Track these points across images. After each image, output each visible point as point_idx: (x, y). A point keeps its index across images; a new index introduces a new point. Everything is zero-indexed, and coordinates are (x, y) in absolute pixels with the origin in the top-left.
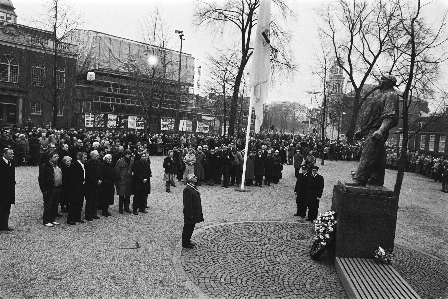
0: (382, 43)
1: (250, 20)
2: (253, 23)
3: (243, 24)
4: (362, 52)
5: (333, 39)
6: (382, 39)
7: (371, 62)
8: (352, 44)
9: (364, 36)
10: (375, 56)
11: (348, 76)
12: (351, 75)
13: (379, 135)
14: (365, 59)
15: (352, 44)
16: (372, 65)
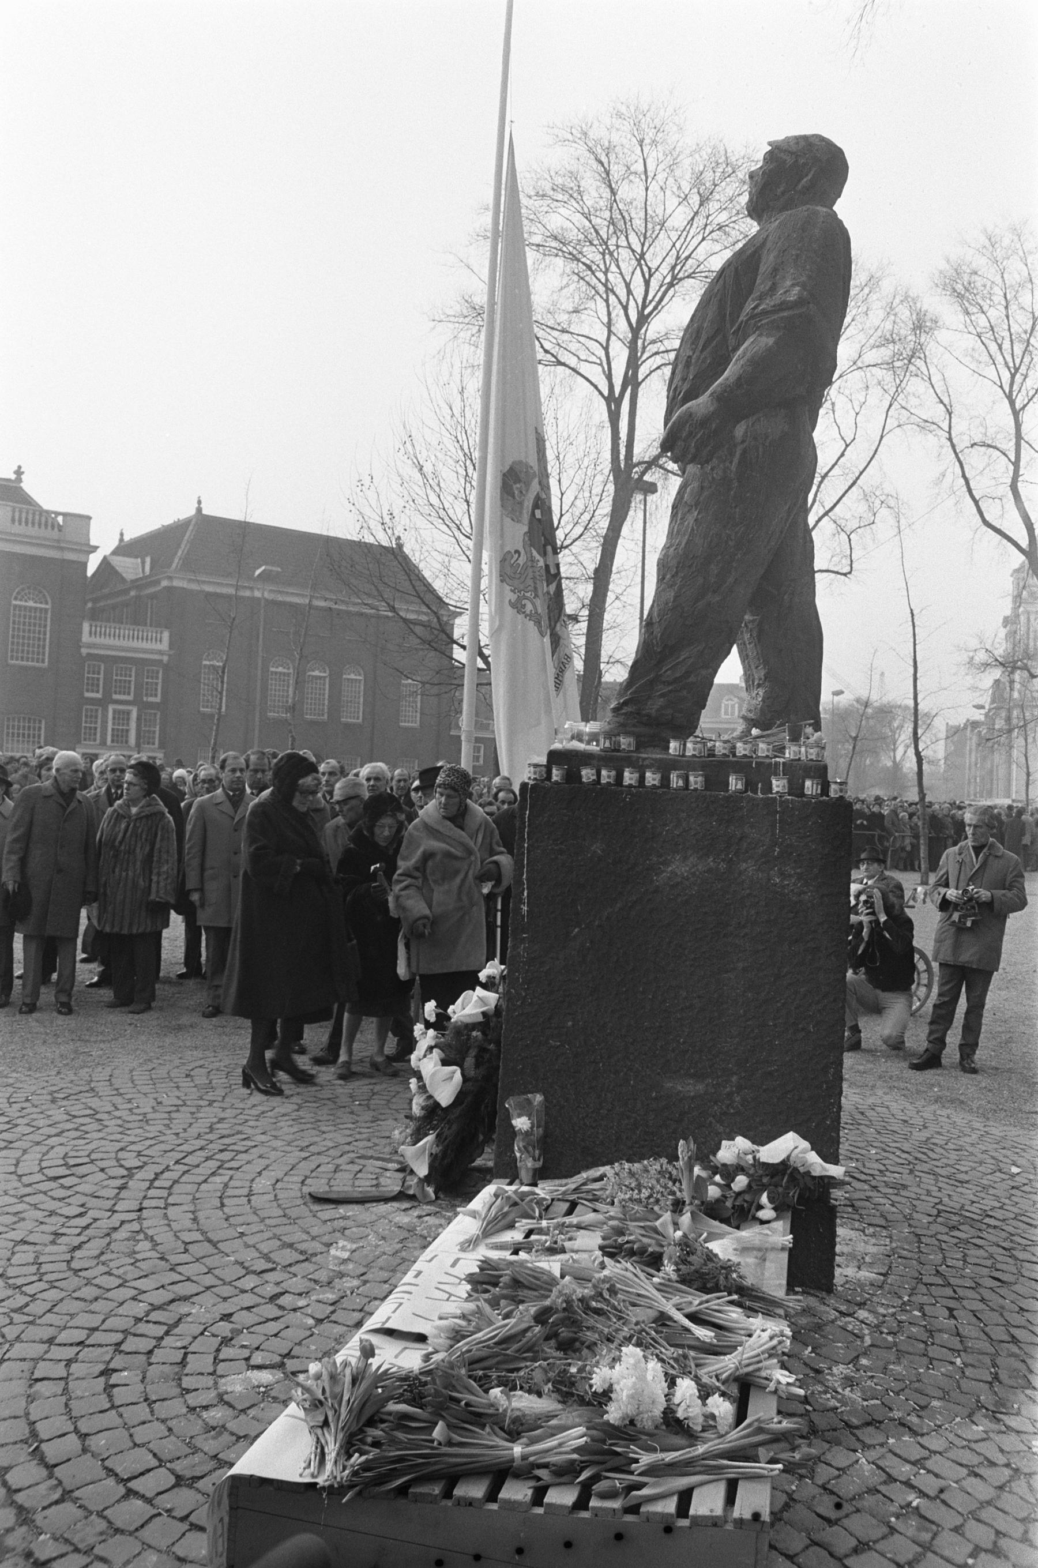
13: (704, 422)
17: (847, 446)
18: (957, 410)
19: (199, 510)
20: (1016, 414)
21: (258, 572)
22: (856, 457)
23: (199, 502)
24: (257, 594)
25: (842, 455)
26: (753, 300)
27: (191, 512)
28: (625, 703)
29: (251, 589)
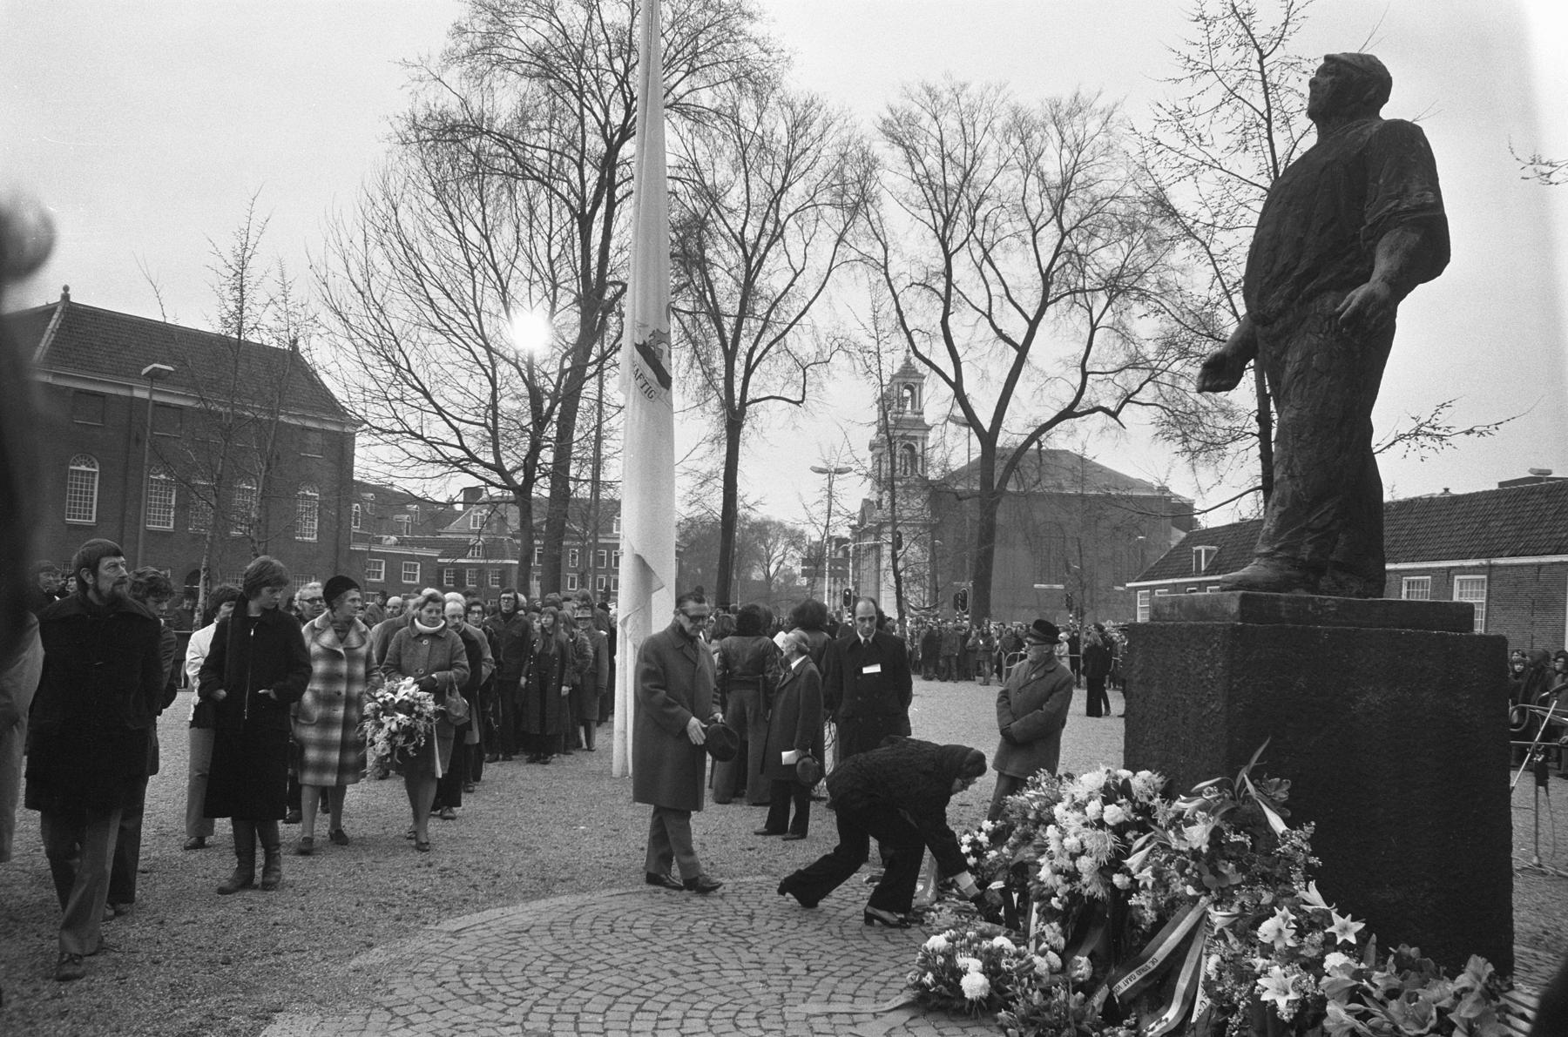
0: (1047, 278)
1: (607, 184)
2: (618, 193)
3: (583, 201)
4: (984, 306)
5: (885, 267)
6: (1045, 264)
7: (1020, 342)
8: (949, 284)
9: (986, 253)
10: (1031, 317)
11: (951, 392)
12: (957, 386)
14: (999, 332)
15: (949, 284)
16: (1023, 351)
17: (797, 275)
18: (891, 246)
19: (66, 297)
20: (948, 257)
21: (145, 371)
22: (808, 285)
23: (66, 288)
24: (138, 394)
25: (791, 284)
26: (1393, 198)
27: (55, 298)
28: (1280, 549)
29: (131, 388)
